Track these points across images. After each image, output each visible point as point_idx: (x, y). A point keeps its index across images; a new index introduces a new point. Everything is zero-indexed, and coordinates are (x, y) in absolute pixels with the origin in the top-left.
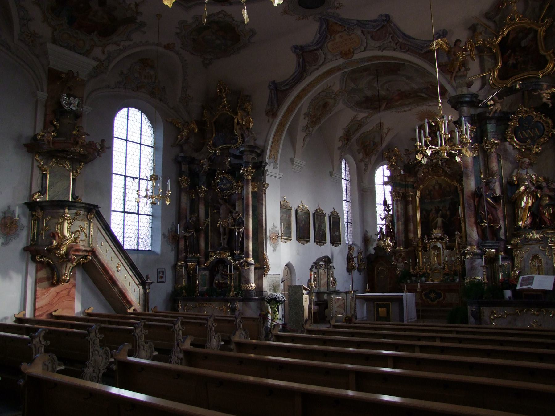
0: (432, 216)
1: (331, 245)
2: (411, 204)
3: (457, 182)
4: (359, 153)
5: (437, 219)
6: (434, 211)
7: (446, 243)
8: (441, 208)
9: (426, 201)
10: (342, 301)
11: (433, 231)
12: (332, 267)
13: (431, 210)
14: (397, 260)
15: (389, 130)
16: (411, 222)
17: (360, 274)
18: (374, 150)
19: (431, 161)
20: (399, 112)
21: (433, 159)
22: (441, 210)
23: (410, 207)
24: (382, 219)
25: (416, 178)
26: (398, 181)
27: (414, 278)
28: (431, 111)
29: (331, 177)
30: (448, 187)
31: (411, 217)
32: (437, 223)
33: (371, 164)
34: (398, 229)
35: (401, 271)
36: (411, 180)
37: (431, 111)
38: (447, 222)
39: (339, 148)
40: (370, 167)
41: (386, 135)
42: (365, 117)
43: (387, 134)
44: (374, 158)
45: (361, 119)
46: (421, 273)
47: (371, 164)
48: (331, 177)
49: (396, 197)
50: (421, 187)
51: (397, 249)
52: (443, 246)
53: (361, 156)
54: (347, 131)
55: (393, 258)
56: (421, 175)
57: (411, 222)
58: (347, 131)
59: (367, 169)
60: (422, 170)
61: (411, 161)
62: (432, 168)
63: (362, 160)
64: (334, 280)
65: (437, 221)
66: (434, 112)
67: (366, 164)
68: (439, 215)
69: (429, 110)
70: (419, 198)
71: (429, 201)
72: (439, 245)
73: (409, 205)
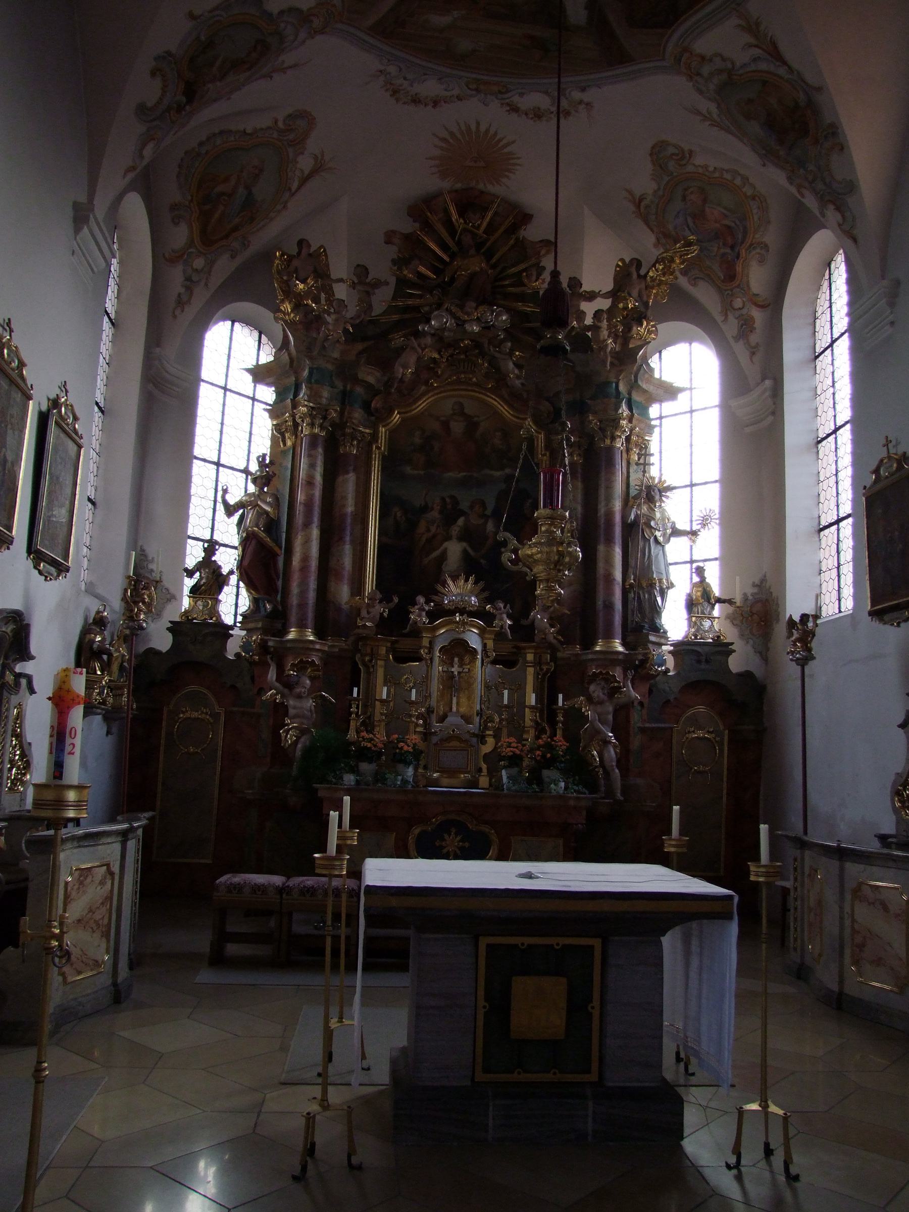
0: (428, 530)
1: (30, 564)
2: (354, 470)
3: (536, 422)
4: (176, 222)
5: (446, 544)
6: (435, 514)
7: (500, 636)
8: (464, 505)
9: (408, 470)
10: (102, 883)
11: (444, 584)
12: (24, 682)
13: (425, 509)
14: (288, 685)
15: (319, 168)
16: (348, 538)
17: (108, 733)
18: (235, 229)
19: (457, 325)
20: (395, 92)
21: (465, 321)
22: (462, 513)
23: (349, 483)
24: (230, 510)
25: (386, 379)
26: (330, 367)
27: (365, 767)
28: (500, 140)
29: (77, 230)
30: (498, 434)
31: (349, 520)
32: (443, 557)
33: (206, 285)
34: (305, 559)
35: (303, 732)
36: (371, 379)
37: (500, 140)
38: (483, 561)
39: (142, 110)
40: (200, 296)
41: (299, 188)
42: (298, 11)
43: (304, 180)
44: (224, 266)
45: (282, 12)
46: (406, 748)
47: (206, 285)
48: (77, 230)
49: (312, 425)
50: (396, 417)
51: (291, 636)
52: (485, 646)
53: (179, 236)
54: (203, 38)
55: (272, 675)
56: (406, 369)
57: (348, 538)
58: (203, 38)
59: (189, 302)
60: (420, 350)
61: (373, 314)
62: (452, 356)
63: (176, 258)
64: (23, 755)
65: (446, 549)
66: (506, 150)
67: (188, 279)
68: (455, 530)
69: (496, 134)
70: (384, 459)
71: (422, 472)
72: (474, 640)
73: (347, 472)
